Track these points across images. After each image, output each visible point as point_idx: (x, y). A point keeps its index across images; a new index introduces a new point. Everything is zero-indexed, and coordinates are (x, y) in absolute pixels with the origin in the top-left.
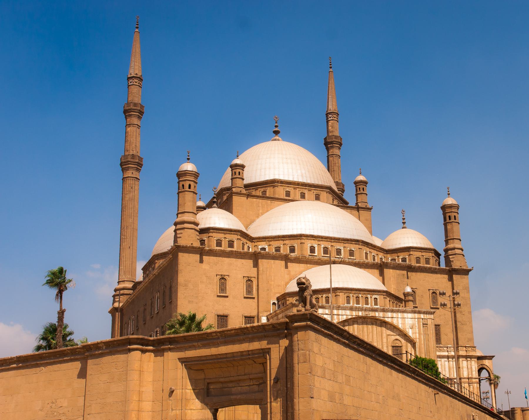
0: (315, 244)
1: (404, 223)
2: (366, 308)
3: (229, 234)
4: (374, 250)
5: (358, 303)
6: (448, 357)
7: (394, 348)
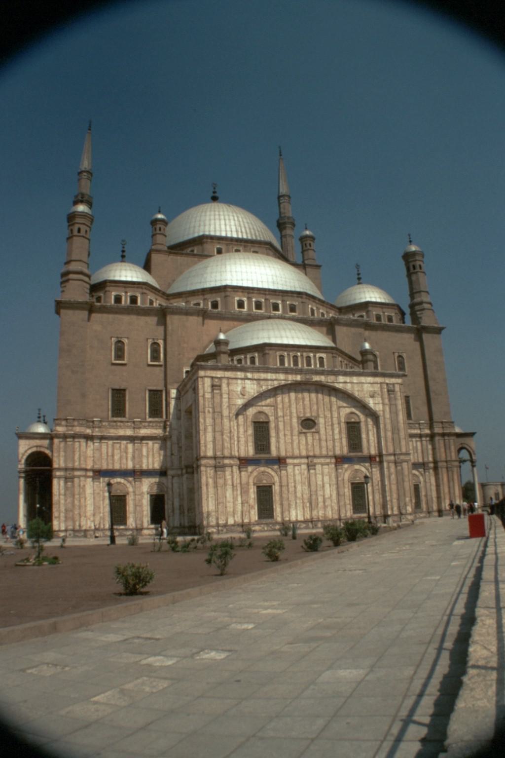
0: (244, 296)
1: (359, 279)
2: (307, 370)
3: (132, 287)
4: (323, 306)
5: (296, 363)
6: (420, 436)
7: (350, 425)
